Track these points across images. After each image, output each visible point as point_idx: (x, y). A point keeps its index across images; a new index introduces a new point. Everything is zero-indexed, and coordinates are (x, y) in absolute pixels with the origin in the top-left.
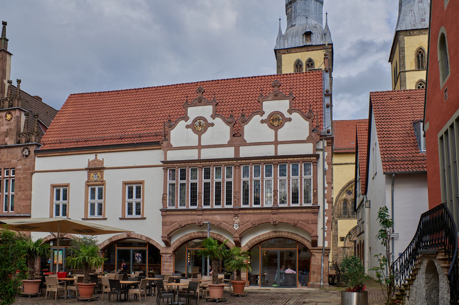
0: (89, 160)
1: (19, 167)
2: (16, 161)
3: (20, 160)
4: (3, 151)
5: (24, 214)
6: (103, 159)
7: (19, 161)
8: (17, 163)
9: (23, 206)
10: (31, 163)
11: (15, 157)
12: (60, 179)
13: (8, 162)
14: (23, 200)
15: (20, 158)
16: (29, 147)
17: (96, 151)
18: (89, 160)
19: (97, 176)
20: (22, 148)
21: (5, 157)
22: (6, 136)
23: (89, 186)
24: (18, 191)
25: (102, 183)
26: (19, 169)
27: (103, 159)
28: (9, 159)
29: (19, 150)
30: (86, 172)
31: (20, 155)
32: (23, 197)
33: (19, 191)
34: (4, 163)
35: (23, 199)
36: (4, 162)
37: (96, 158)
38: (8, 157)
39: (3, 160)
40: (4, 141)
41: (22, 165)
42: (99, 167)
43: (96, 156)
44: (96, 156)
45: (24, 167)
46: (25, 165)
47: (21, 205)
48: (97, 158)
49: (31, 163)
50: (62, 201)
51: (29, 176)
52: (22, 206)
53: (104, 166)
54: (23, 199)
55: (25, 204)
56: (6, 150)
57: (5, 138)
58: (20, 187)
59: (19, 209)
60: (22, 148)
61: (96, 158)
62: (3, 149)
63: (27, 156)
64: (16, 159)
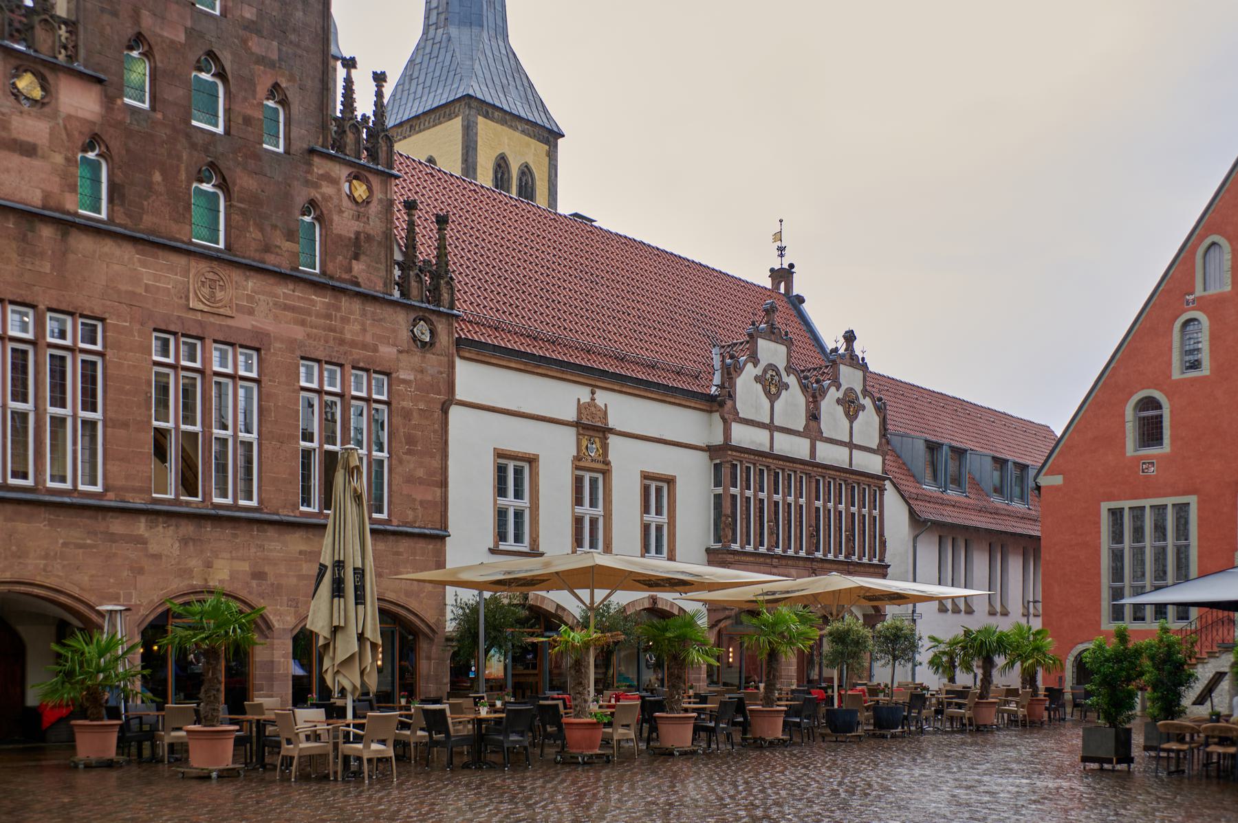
0: (579, 400)
1: (403, 375)
2: (395, 350)
3: (407, 352)
4: (347, 304)
5: (424, 528)
6: (606, 405)
7: (405, 355)
8: (398, 360)
9: (421, 503)
10: (442, 373)
11: (389, 338)
12: (520, 438)
13: (365, 346)
14: (420, 484)
15: (405, 347)
16: (434, 318)
17: (593, 383)
18: (579, 400)
19: (594, 446)
20: (412, 316)
21: (357, 327)
22: (356, 257)
23: (578, 468)
24: (404, 453)
25: (606, 468)
26: (404, 381)
27: (606, 405)
28: (368, 338)
29: (401, 319)
30: (571, 433)
31: (404, 335)
32: (420, 473)
33: (409, 452)
34: (351, 347)
35: (421, 481)
36: (353, 344)
37: (593, 399)
38: (364, 330)
39: (348, 336)
40: (350, 270)
41: (413, 369)
42: (600, 424)
43: (593, 393)
44: (593, 393)
45: (419, 376)
46: (422, 372)
47: (414, 500)
48: (594, 400)
49: (442, 370)
50: (513, 499)
51: (438, 414)
52: (417, 503)
53: (610, 426)
54: (421, 481)
55: (430, 498)
56: (357, 305)
57: (350, 263)
58: (410, 440)
59: (410, 512)
60: (412, 316)
61: (593, 399)
62: (347, 298)
63: (424, 344)
64: (394, 345)
